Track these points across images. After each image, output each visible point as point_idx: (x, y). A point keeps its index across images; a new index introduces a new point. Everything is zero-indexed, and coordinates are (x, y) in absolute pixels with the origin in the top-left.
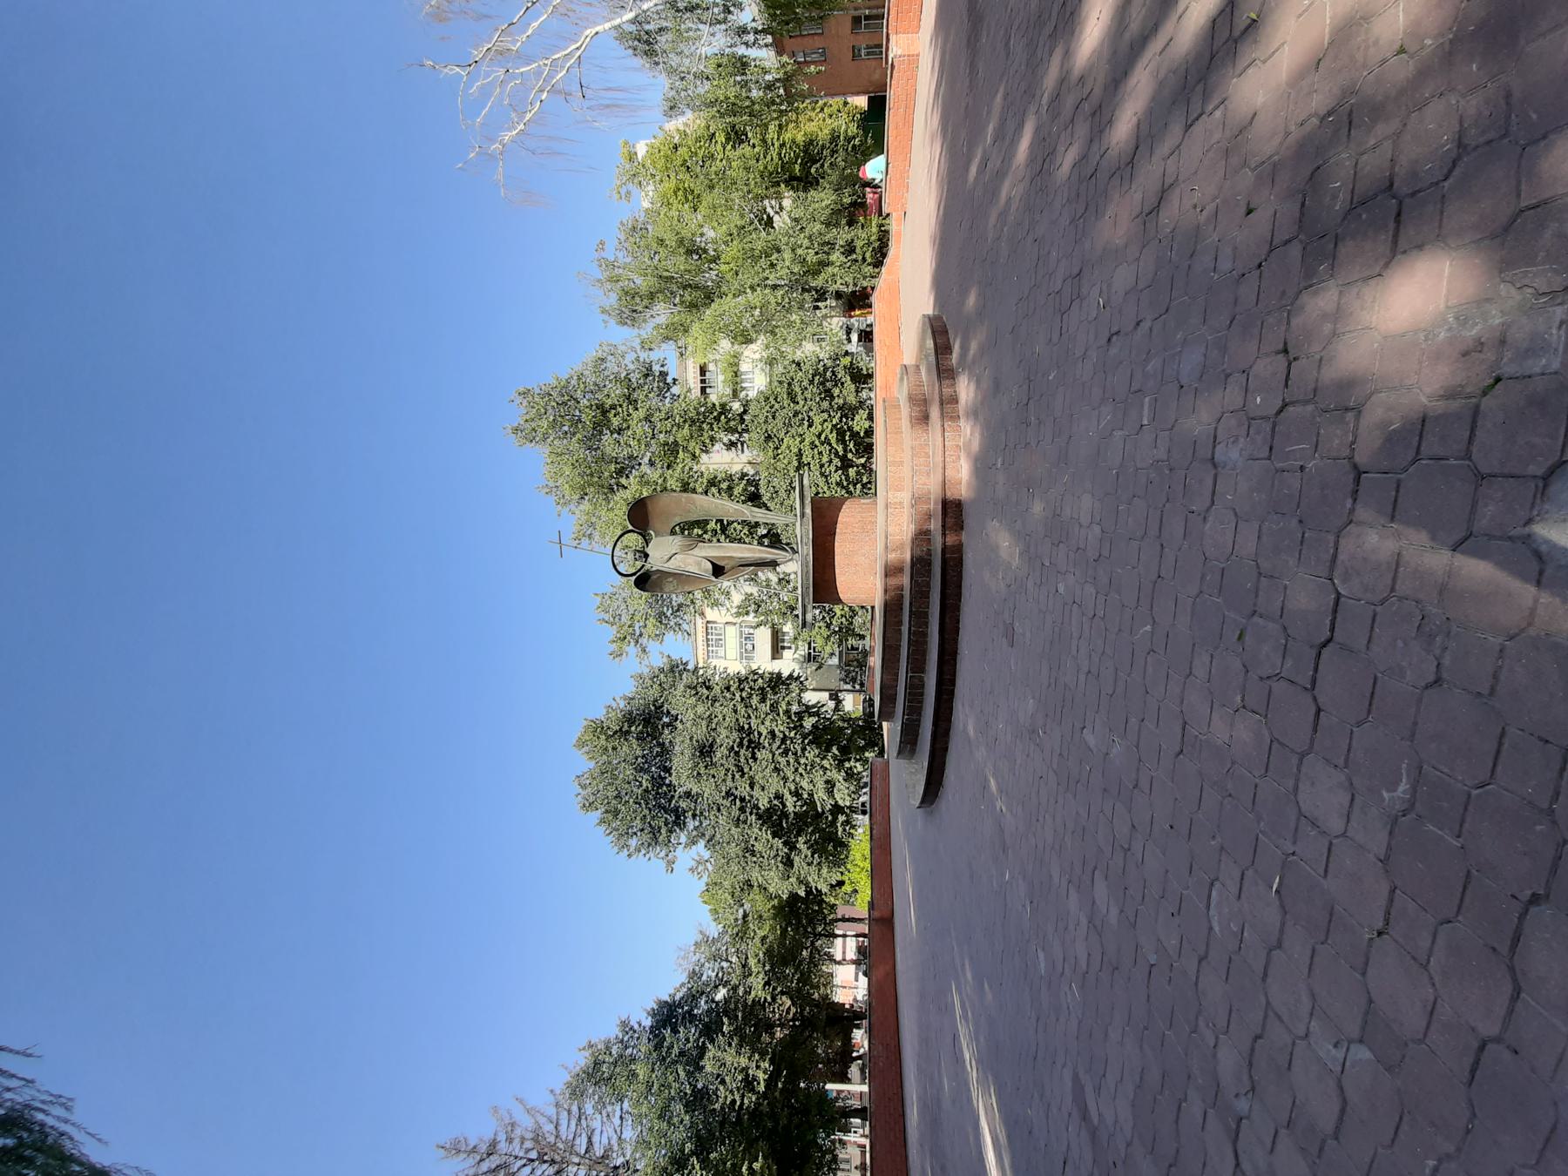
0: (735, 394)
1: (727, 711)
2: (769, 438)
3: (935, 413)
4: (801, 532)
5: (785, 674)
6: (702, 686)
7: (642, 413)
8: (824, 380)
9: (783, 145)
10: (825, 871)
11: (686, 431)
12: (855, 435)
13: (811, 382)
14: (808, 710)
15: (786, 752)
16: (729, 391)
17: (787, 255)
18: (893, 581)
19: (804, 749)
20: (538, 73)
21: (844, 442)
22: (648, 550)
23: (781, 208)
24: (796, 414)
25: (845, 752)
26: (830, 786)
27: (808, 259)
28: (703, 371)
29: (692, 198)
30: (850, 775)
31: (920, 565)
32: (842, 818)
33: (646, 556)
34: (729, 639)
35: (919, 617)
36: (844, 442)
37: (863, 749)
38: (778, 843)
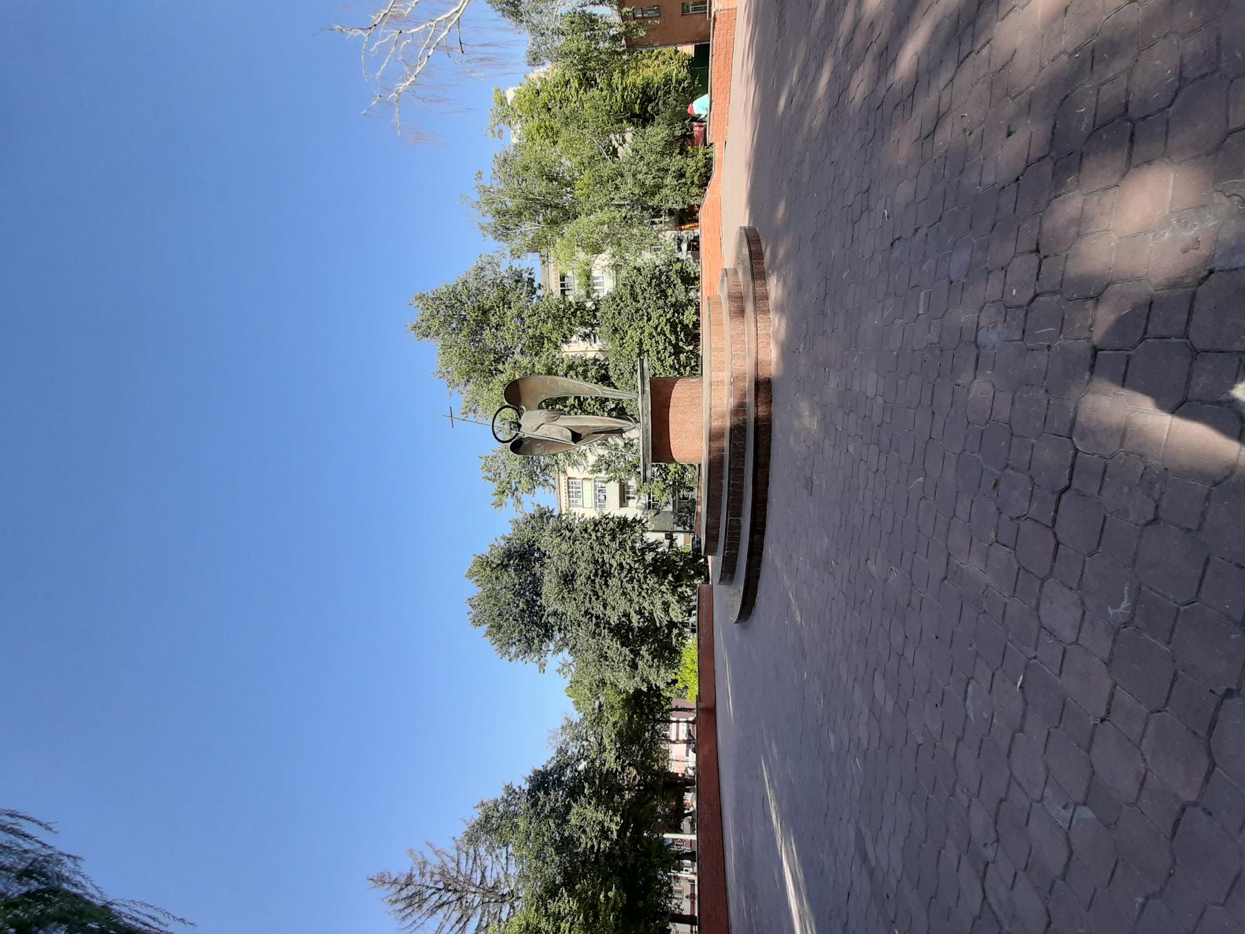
0: (588, 295)
1: (586, 548)
2: (616, 331)
3: (749, 307)
4: (642, 405)
5: (630, 518)
6: (565, 529)
7: (514, 311)
8: (660, 282)
9: (625, 89)
10: (662, 671)
11: (550, 325)
12: (685, 327)
13: (650, 284)
14: (651, 547)
15: (631, 580)
16: (583, 292)
17: (630, 180)
18: (715, 445)
19: (645, 578)
20: (426, 32)
21: (676, 333)
22: (521, 422)
23: (624, 141)
24: (637, 311)
25: (678, 579)
26: (666, 606)
27: (647, 182)
28: (562, 278)
29: (552, 135)
30: (682, 598)
31: (737, 431)
32: (675, 631)
33: (520, 426)
34: (586, 491)
35: (737, 472)
36: (676, 333)
37: (692, 578)
38: (626, 651)
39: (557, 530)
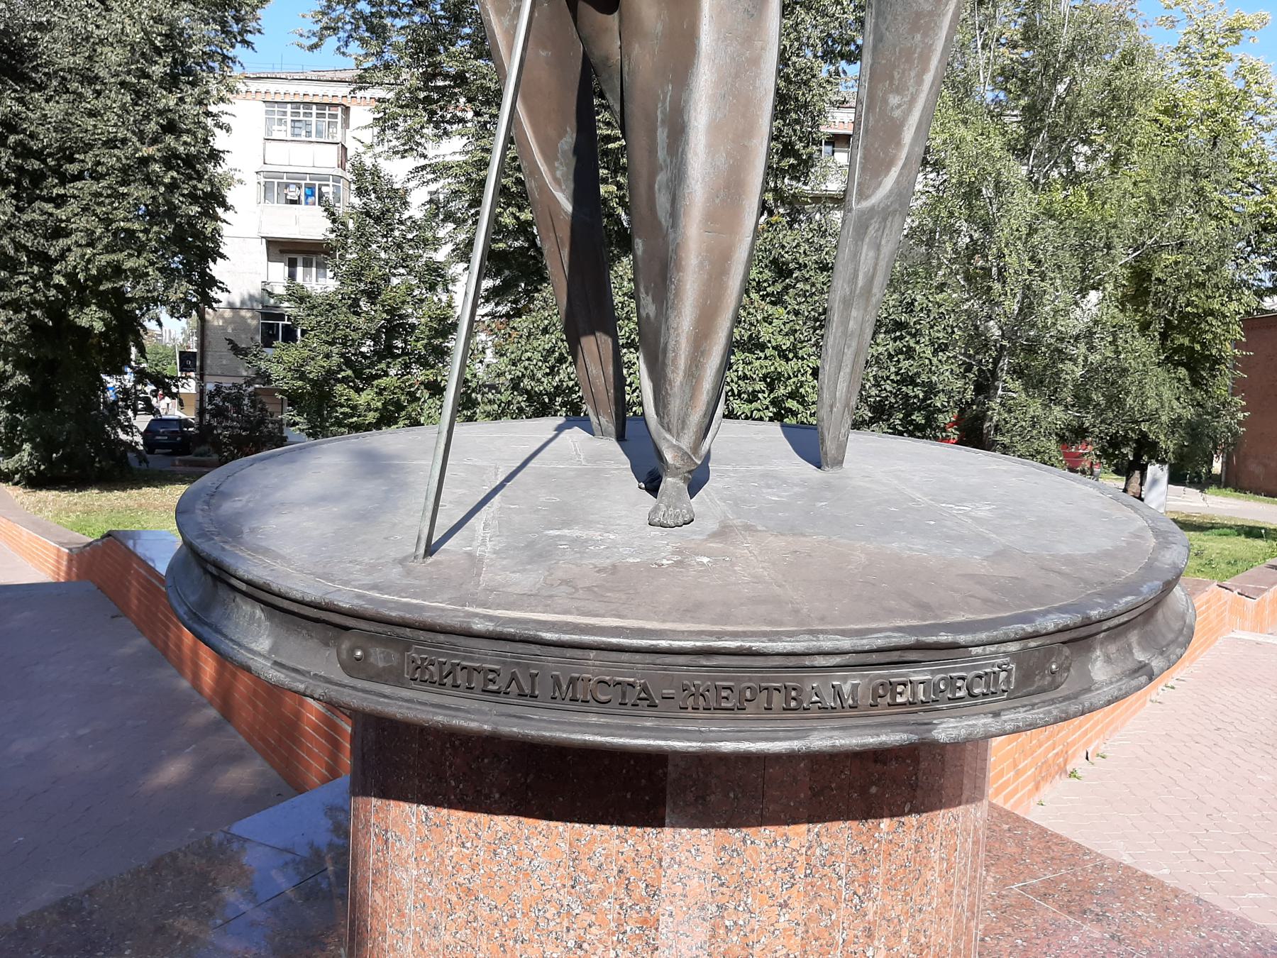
1: (110, 125)
5: (217, 269)
13: (910, 380)
14: (126, 328)
19: (16, 306)
39: (174, 40)
